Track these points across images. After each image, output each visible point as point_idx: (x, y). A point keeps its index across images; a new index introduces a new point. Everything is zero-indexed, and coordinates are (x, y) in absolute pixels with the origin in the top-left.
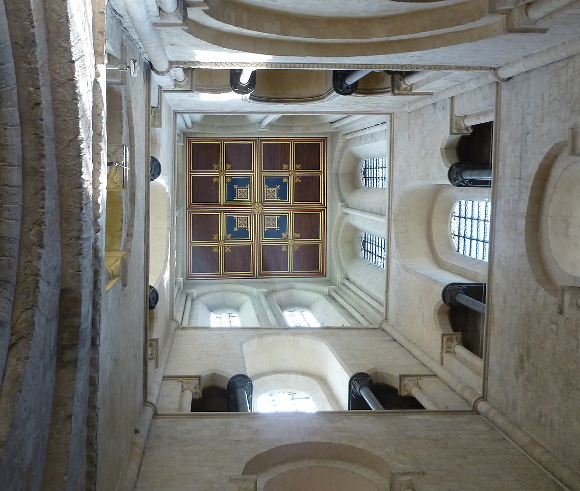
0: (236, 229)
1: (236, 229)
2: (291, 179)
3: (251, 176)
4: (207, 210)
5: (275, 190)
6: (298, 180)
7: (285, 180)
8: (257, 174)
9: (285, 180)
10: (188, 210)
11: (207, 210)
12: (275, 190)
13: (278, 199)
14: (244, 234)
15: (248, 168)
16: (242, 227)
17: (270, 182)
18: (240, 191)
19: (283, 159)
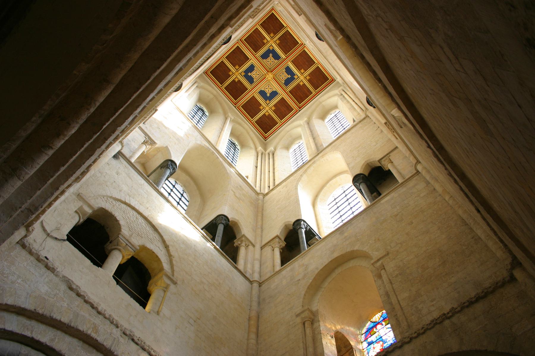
0: (268, 95)
1: (268, 95)
2: (274, 45)
3: (252, 62)
4: (245, 98)
5: (271, 59)
6: (278, 42)
7: (271, 48)
8: (253, 59)
9: (271, 48)
10: (236, 107)
11: (245, 98)
12: (271, 59)
13: (276, 61)
14: (274, 94)
15: (247, 59)
16: (270, 91)
17: (265, 56)
18: (253, 74)
19: (261, 39)
